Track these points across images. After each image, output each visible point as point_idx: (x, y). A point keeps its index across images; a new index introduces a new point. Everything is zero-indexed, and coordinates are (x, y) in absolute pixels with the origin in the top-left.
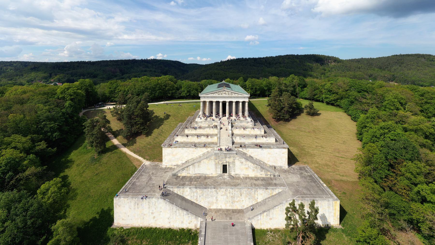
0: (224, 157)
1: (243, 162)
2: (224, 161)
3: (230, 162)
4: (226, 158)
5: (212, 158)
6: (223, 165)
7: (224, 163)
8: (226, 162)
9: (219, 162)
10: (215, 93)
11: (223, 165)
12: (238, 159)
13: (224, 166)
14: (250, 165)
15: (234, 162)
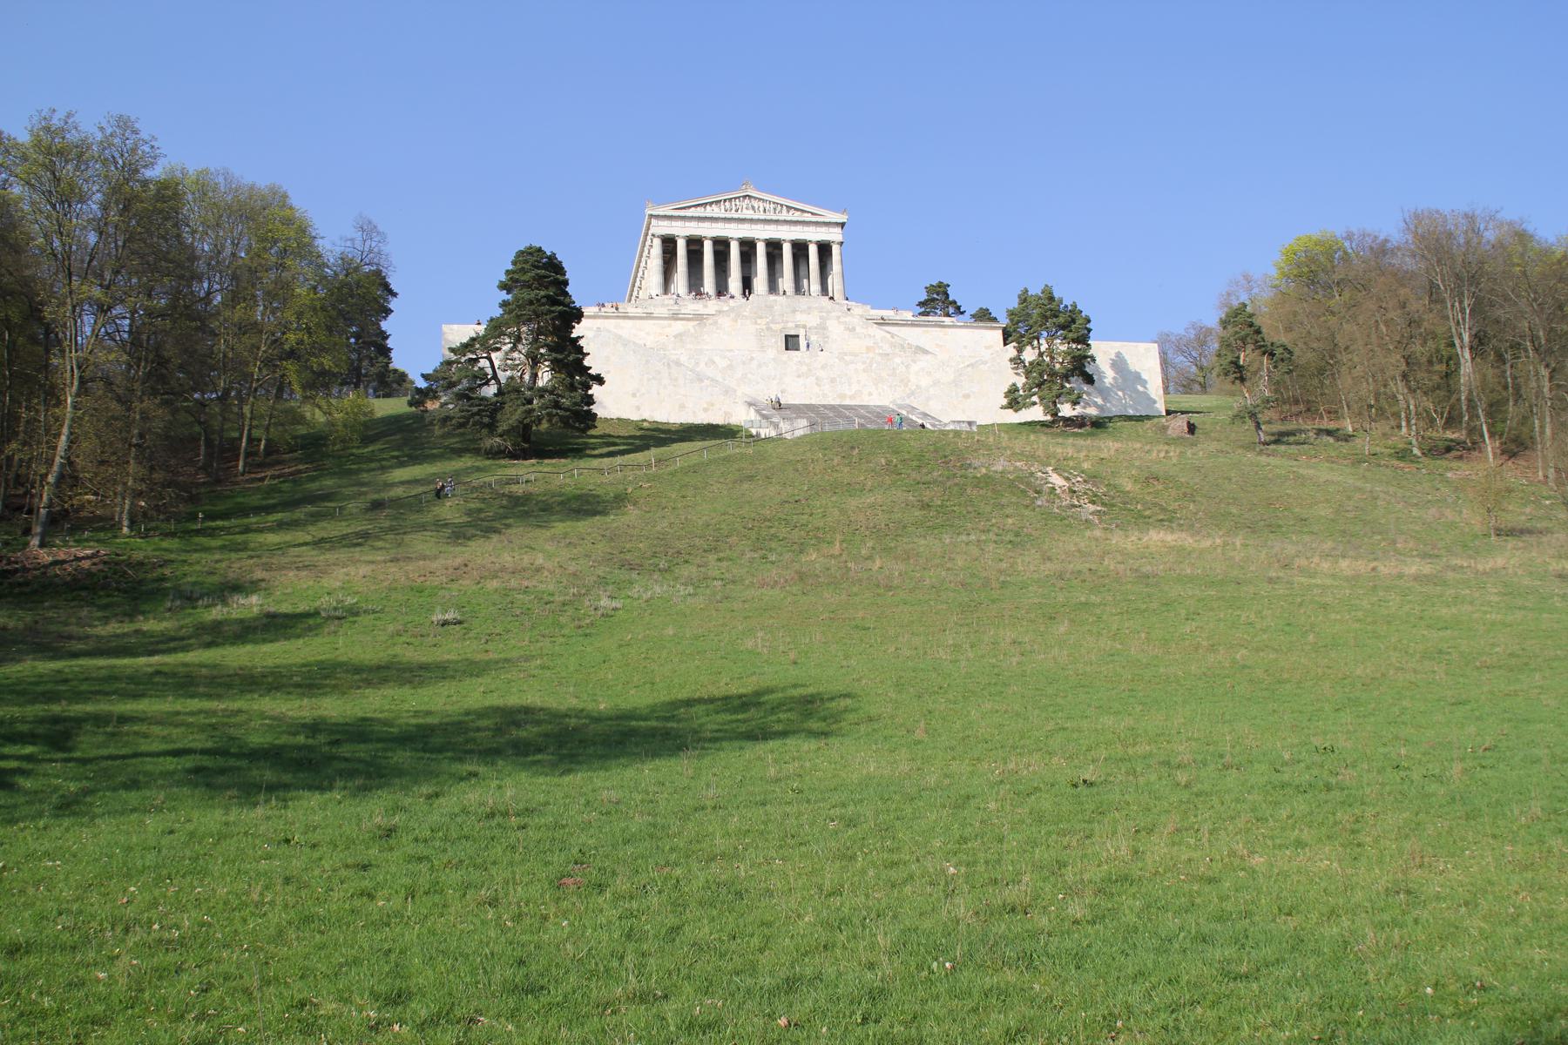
1: (854, 329)
2: (787, 322)
3: (808, 325)
4: (794, 311)
6: (786, 336)
7: (791, 329)
8: (797, 326)
9: (771, 325)
10: (711, 203)
11: (786, 336)
12: (839, 317)
13: (790, 339)
15: (822, 328)
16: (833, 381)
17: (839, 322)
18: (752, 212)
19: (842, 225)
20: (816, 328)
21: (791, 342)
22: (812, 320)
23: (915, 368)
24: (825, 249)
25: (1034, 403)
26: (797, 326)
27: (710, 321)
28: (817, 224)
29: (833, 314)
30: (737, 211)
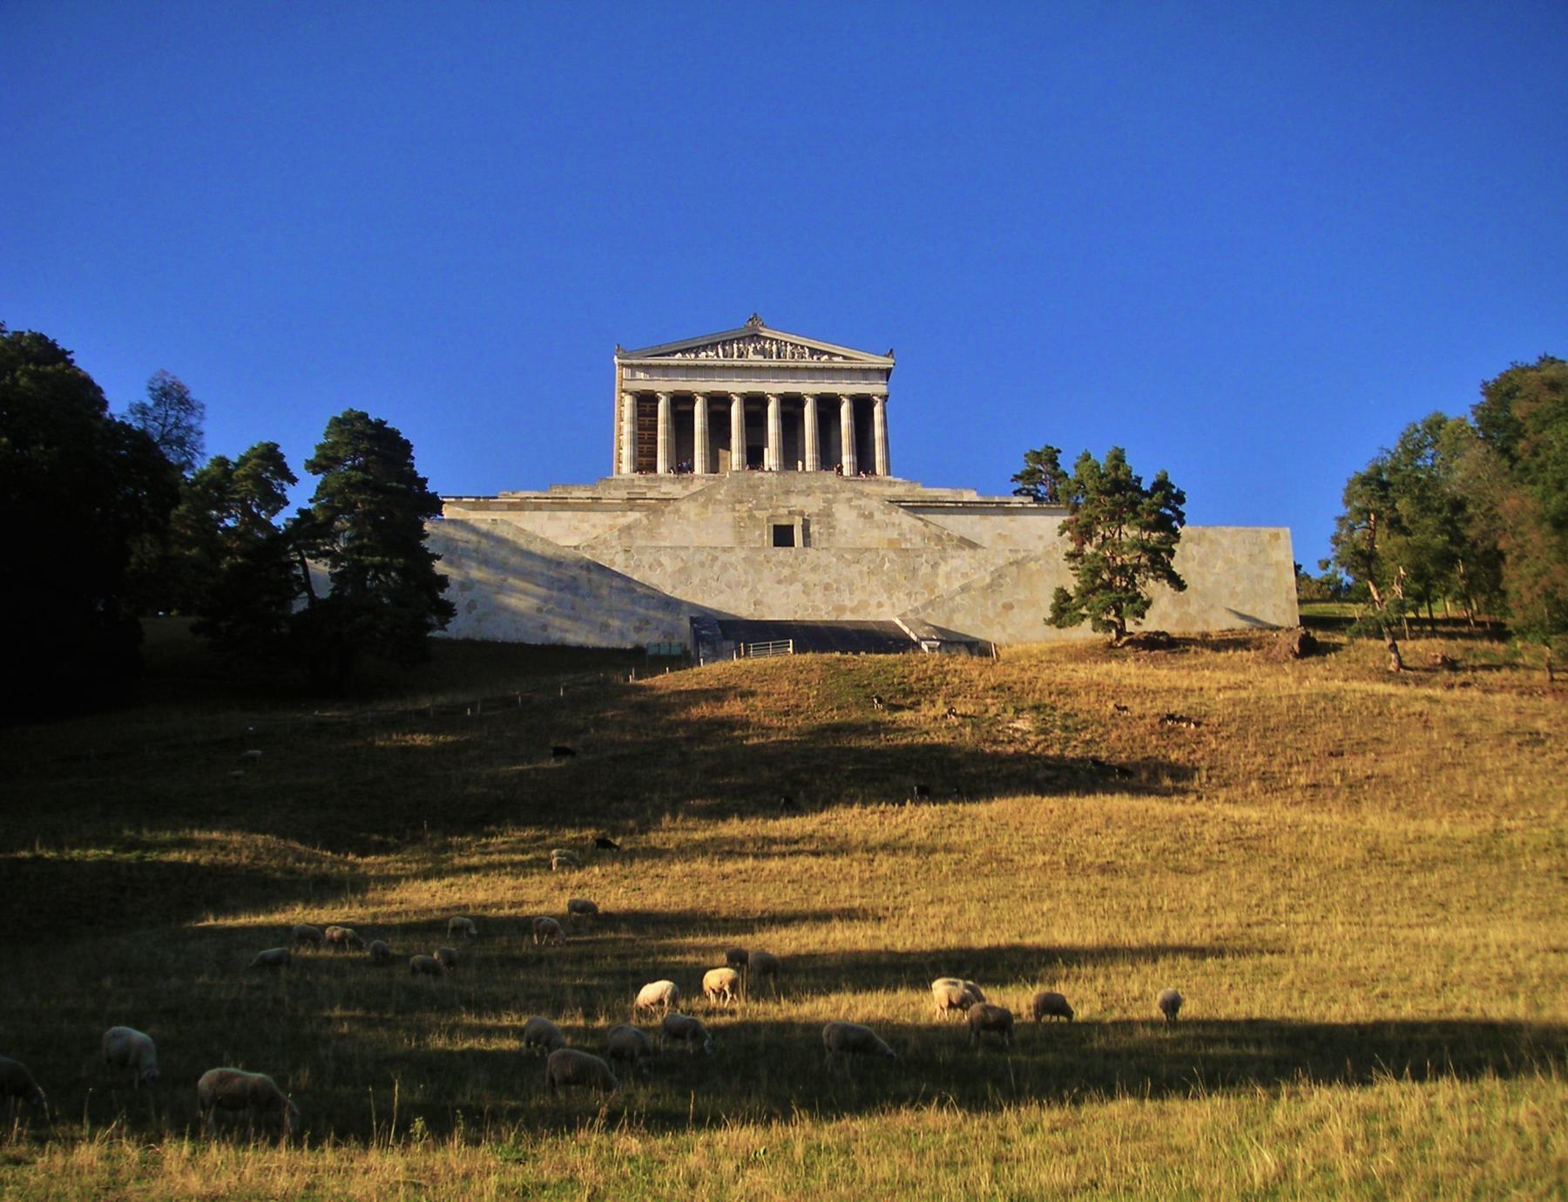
0: (779, 491)
1: (871, 515)
2: (778, 507)
4: (788, 492)
5: (719, 497)
6: (775, 527)
7: (781, 516)
8: (790, 513)
9: (757, 513)
10: (705, 348)
11: (775, 527)
12: (850, 500)
14: (905, 526)
15: (827, 514)
16: (827, 587)
17: (851, 506)
18: (760, 357)
19: (886, 373)
20: (818, 515)
21: (783, 536)
22: (812, 505)
23: (943, 569)
24: (863, 406)
25: (1084, 616)
26: (790, 513)
27: (670, 508)
28: (851, 370)
29: (843, 495)
30: (740, 356)
